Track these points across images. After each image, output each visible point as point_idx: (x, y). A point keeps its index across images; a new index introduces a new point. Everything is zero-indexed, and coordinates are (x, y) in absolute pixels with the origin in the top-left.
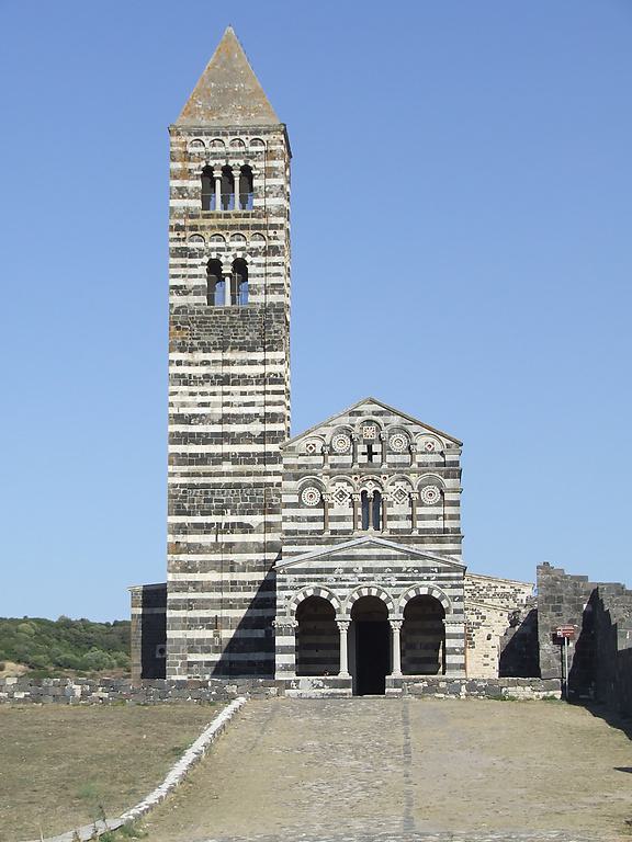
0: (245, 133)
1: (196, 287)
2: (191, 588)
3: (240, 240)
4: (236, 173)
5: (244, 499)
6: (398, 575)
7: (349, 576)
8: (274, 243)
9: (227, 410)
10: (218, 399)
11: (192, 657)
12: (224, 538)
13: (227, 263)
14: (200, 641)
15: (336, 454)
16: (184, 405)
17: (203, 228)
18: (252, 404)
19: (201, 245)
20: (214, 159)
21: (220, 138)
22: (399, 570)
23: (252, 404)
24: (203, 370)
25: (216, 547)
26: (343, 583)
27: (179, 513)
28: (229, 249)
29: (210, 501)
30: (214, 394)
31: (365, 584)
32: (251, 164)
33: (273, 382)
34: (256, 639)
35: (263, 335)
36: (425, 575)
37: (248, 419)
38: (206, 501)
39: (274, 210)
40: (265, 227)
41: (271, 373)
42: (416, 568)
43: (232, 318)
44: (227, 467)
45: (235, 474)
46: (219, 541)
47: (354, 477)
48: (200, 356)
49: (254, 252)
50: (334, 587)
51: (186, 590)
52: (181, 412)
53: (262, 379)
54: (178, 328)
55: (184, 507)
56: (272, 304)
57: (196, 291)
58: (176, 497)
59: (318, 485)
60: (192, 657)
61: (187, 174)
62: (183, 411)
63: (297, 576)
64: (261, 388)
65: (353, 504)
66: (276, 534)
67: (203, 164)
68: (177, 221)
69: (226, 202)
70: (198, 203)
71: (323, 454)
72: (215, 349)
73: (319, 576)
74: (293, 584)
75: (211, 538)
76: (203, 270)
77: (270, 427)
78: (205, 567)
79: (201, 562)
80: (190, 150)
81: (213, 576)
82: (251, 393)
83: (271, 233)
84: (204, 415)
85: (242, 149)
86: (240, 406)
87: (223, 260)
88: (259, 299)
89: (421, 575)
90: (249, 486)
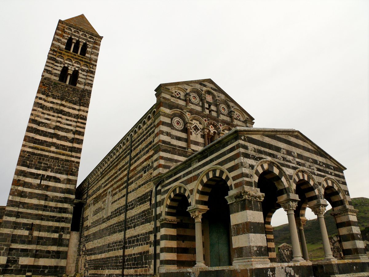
0: (88, 34)
1: (55, 73)
2: (21, 206)
3: (78, 64)
4: (81, 44)
5: (59, 166)
8: (92, 69)
9: (58, 124)
10: (55, 119)
11: (14, 246)
12: (44, 183)
13: (71, 70)
14: (20, 236)
15: (192, 103)
16: (38, 116)
17: (64, 54)
18: (70, 125)
19: (62, 60)
20: (74, 36)
21: (78, 31)
23: (70, 125)
24: (51, 105)
25: (39, 186)
26: (288, 163)
27: (23, 165)
28: (73, 66)
29: (41, 163)
30: (53, 116)
31: (301, 168)
32: (88, 43)
33: (82, 118)
34: (53, 238)
35: (80, 100)
37: (68, 131)
38: (39, 162)
39: (94, 59)
40: (89, 63)
41: (81, 115)
43: (68, 89)
44: (53, 149)
45: (57, 153)
46: (42, 183)
47: (204, 119)
48: (50, 99)
49: (83, 70)
50: (283, 165)
51: (18, 207)
52: (36, 119)
53: (77, 116)
54: (44, 85)
55: (27, 163)
56: (86, 89)
57: (55, 75)
58: (24, 157)
59: (181, 116)
60: (14, 246)
61: (63, 37)
62: (37, 118)
64: (75, 120)
65: (203, 136)
66: (72, 186)
67: (69, 36)
68: (54, 49)
69: (76, 50)
70: (64, 47)
71: (185, 100)
72: (59, 99)
75: (38, 181)
76: (60, 69)
77: (77, 136)
78: (31, 195)
79: (30, 193)
80: (66, 30)
81: (35, 201)
82: (71, 121)
83: (91, 66)
84: (47, 123)
85: (85, 38)
86: (64, 124)
87: (69, 68)
88: (82, 86)
89: (327, 170)
90: (62, 160)
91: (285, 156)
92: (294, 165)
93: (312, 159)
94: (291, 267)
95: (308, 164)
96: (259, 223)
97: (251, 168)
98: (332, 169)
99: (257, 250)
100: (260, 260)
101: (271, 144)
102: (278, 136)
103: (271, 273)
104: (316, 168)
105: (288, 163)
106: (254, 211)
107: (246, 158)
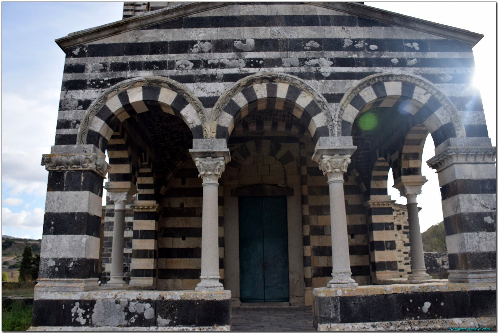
6: (334, 54)
7: (225, 57)
22: (336, 44)
26: (211, 71)
36: (395, 56)
42: (370, 41)
50: (189, 79)
63: (111, 59)
73: (156, 58)
74: (98, 75)
89: (386, 55)
91: (205, 56)
92: (235, 71)
93: (316, 40)
94: (149, 301)
95: (294, 56)
96: (73, 214)
97: (81, 107)
98: (413, 50)
99: (56, 266)
100: (57, 284)
101: (162, 40)
102: (195, 15)
103: (81, 311)
104: (331, 60)
105: (211, 71)
106: (67, 190)
107: (73, 91)
